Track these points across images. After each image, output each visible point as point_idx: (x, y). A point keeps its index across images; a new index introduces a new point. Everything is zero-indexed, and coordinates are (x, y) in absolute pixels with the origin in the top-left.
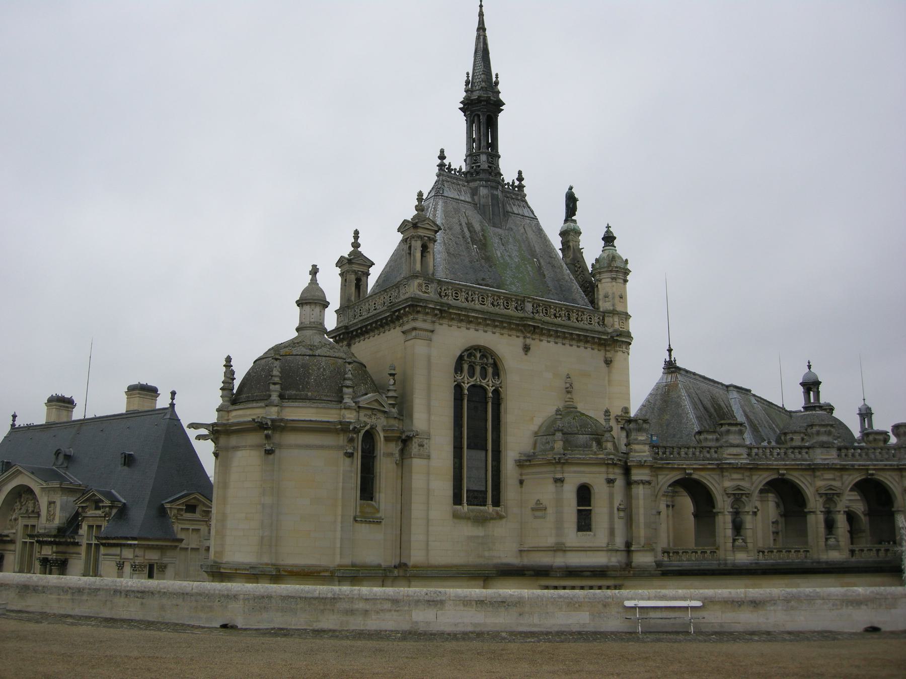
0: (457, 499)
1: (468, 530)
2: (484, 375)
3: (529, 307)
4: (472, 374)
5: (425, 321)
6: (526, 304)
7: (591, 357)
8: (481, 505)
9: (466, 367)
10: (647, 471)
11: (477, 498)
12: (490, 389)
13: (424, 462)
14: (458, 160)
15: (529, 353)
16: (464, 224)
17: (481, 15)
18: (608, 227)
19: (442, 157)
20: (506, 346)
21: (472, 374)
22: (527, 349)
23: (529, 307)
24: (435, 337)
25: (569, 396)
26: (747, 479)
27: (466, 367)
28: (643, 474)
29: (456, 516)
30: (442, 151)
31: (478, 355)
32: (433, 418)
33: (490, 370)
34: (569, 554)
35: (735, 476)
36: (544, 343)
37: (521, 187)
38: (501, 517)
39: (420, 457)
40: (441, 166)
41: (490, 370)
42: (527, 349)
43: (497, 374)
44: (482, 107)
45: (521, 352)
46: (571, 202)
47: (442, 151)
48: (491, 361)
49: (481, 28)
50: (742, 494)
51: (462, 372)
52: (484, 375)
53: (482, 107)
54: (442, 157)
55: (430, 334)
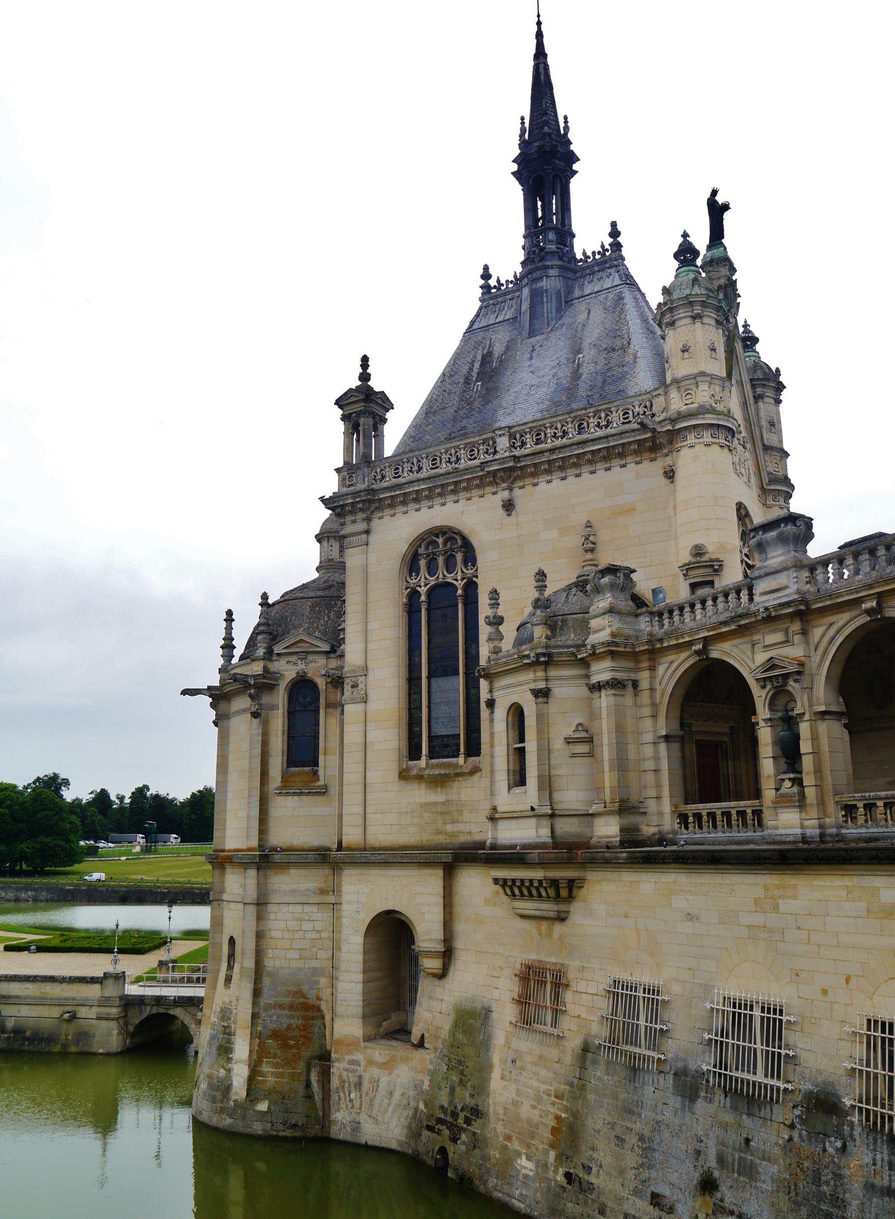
0: (414, 752)
1: (420, 794)
2: (450, 566)
3: (503, 442)
4: (432, 569)
5: (354, 522)
6: (498, 440)
7: (635, 478)
8: (453, 757)
9: (423, 563)
10: (607, 663)
11: (443, 747)
12: (460, 584)
13: (360, 707)
14: (508, 264)
15: (514, 513)
16: (479, 357)
17: (539, 35)
18: (685, 235)
19: (486, 275)
20: (473, 514)
21: (432, 569)
22: (509, 506)
23: (503, 442)
24: (373, 538)
25: (589, 556)
26: (797, 638)
27: (423, 563)
28: (604, 670)
29: (404, 775)
30: (486, 268)
31: (440, 541)
32: (371, 646)
33: (459, 557)
34: (502, 824)
35: (773, 638)
36: (543, 486)
37: (617, 246)
38: (475, 770)
39: (353, 701)
40: (486, 288)
41: (459, 557)
42: (509, 506)
43: (470, 558)
44: (545, 162)
45: (501, 512)
46: (717, 211)
47: (486, 268)
48: (460, 542)
49: (540, 55)
50: (786, 676)
51: (418, 572)
52: (450, 566)
53: (545, 162)
54: (486, 275)
55: (364, 536)
